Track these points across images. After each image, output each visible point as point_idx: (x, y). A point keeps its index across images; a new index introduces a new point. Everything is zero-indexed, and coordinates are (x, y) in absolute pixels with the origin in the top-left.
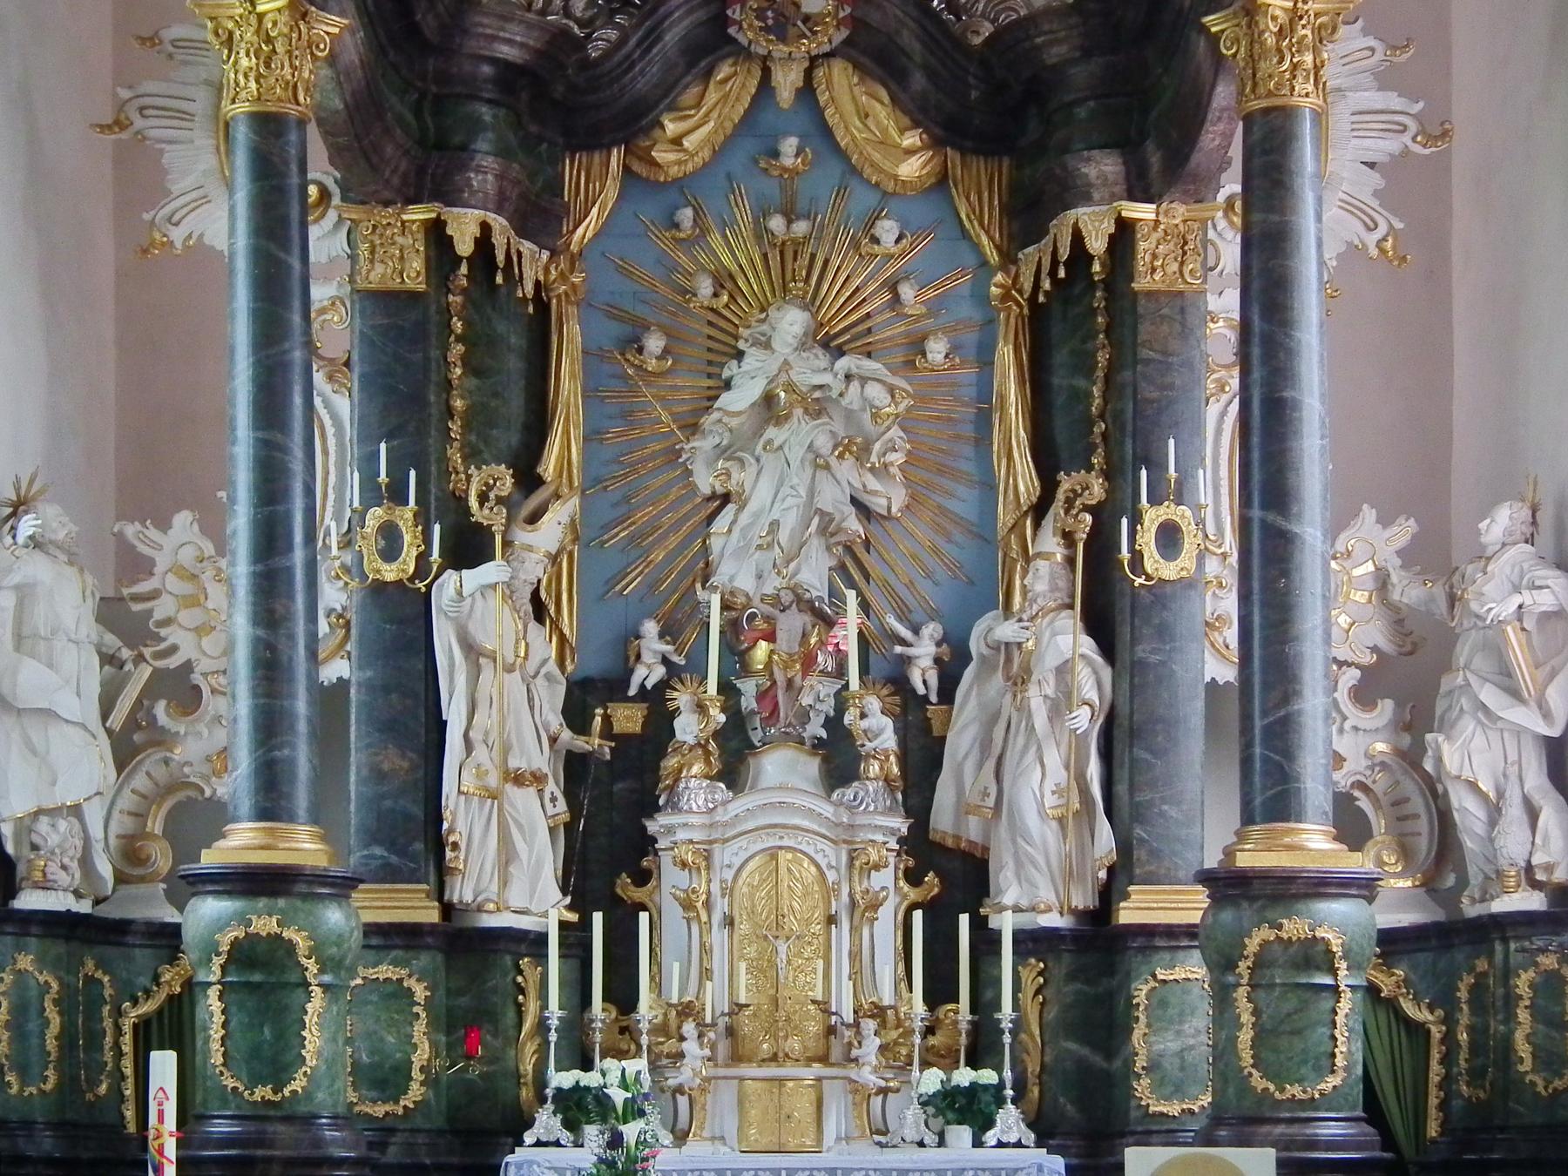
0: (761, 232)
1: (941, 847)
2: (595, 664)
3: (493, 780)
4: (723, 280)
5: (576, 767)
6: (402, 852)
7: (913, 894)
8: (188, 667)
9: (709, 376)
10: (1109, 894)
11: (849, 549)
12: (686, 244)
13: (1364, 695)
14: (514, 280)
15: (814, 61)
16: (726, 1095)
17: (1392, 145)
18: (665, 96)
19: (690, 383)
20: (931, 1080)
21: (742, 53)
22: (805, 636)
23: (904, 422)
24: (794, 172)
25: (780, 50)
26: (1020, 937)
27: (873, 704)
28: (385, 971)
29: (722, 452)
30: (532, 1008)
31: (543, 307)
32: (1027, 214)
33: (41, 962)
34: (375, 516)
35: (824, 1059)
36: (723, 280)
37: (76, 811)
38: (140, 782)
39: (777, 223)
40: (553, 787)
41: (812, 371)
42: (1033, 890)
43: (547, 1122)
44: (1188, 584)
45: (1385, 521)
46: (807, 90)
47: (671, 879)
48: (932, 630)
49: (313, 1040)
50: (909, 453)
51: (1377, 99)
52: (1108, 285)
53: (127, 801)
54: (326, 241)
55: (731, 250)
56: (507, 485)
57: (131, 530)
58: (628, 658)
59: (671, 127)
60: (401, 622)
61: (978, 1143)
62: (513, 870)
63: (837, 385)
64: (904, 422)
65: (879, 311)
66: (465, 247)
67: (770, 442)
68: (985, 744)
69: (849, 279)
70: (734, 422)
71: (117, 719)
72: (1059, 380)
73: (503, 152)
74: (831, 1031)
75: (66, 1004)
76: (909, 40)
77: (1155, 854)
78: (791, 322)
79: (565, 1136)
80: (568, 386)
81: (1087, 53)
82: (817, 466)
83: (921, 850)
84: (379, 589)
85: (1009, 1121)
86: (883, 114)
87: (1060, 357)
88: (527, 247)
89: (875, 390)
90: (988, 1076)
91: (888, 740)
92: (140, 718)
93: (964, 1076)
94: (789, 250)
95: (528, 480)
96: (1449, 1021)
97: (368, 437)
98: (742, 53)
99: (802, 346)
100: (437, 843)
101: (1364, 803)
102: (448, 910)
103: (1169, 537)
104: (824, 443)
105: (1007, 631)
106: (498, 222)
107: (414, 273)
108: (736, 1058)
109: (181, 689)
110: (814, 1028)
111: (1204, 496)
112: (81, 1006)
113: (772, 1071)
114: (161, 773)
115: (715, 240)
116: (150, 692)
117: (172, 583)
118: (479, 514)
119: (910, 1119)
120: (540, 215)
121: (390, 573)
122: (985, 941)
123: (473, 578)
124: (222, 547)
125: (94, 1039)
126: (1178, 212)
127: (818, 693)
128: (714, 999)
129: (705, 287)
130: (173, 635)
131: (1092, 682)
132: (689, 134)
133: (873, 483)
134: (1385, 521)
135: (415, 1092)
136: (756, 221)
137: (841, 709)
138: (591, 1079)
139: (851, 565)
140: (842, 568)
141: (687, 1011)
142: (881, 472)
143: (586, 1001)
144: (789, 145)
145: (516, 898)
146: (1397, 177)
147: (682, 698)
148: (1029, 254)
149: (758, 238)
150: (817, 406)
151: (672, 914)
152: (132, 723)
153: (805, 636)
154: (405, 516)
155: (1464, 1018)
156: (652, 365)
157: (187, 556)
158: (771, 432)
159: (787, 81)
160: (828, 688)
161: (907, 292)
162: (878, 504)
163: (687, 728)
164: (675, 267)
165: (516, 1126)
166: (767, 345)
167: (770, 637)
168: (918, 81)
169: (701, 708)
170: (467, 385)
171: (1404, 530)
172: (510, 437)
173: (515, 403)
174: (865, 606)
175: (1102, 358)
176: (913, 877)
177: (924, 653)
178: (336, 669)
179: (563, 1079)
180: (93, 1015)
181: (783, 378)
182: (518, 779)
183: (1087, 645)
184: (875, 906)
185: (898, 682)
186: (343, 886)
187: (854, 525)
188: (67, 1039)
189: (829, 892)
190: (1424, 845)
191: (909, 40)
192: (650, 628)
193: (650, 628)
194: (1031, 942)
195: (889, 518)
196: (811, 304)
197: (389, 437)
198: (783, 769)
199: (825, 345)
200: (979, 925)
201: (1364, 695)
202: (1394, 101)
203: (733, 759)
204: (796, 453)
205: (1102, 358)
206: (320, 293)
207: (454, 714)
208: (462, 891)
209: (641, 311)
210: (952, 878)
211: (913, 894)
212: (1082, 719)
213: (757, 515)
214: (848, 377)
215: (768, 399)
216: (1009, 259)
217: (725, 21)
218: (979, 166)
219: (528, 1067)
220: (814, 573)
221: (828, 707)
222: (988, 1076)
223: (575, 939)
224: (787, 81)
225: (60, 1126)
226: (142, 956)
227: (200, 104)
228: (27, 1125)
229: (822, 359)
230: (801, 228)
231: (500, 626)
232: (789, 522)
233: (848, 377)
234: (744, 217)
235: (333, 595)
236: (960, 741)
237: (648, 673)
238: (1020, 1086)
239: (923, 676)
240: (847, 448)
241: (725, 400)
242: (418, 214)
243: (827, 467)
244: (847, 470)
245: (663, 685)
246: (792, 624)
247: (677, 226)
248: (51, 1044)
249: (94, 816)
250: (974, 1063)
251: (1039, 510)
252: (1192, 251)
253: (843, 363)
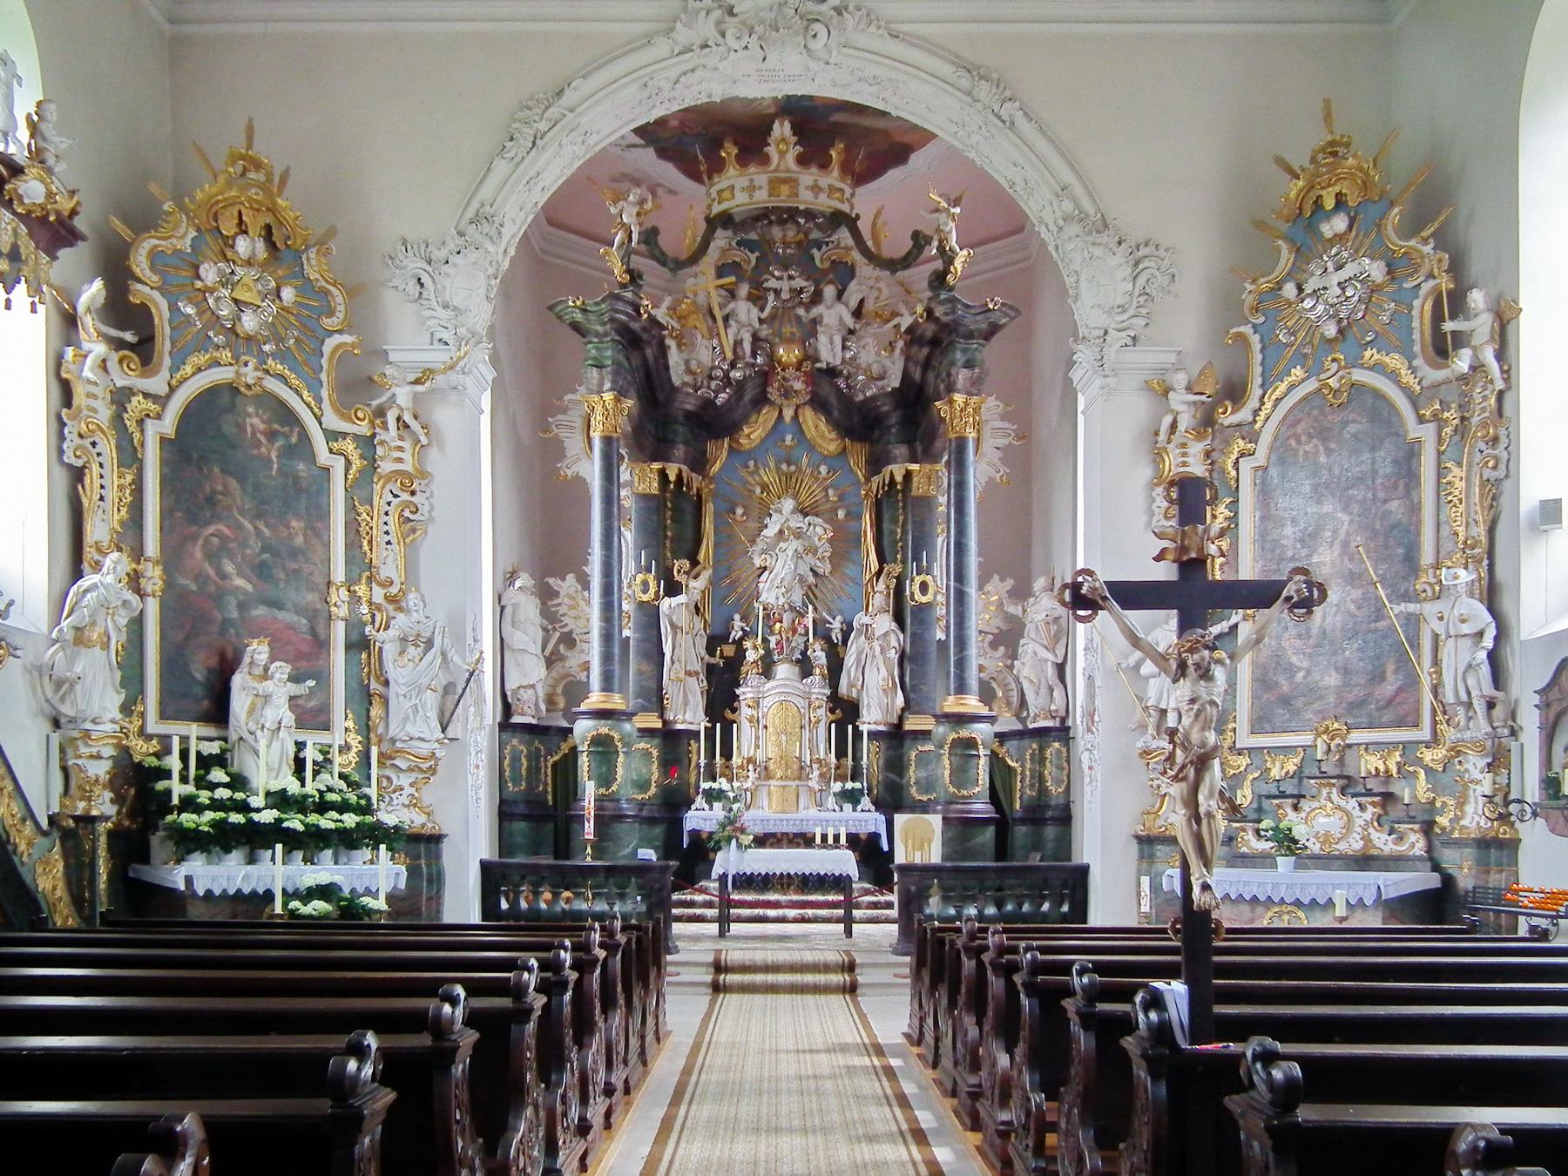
0: (778, 469)
1: (842, 699)
2: (718, 630)
3: (682, 674)
4: (765, 487)
5: (710, 669)
6: (649, 701)
7: (832, 717)
8: (571, 632)
10: (901, 718)
12: (751, 474)
13: (994, 645)
14: (689, 488)
15: (798, 407)
16: (765, 792)
17: (1005, 441)
18: (745, 419)
19: (752, 525)
20: (837, 787)
21: (772, 403)
23: (830, 541)
24: (791, 447)
25: (785, 403)
26: (869, 733)
27: (817, 646)
28: (642, 745)
30: (694, 758)
31: (699, 496)
32: (875, 464)
33: (520, 742)
34: (640, 577)
35: (800, 778)
36: (765, 487)
37: (533, 686)
38: (554, 674)
39: (784, 467)
40: (701, 676)
41: (797, 522)
42: (872, 718)
43: (700, 801)
44: (929, 605)
45: (1002, 580)
46: (796, 417)
47: (745, 711)
48: (839, 618)
49: (620, 770)
51: (1000, 424)
52: (903, 491)
53: (550, 681)
54: (625, 476)
55: (768, 476)
56: (686, 564)
57: (551, 581)
58: (729, 629)
59: (746, 431)
60: (650, 616)
61: (854, 810)
62: (689, 713)
64: (830, 541)
66: (672, 478)
68: (858, 660)
69: (810, 490)
71: (547, 653)
72: (886, 526)
73: (686, 443)
74: (802, 768)
75: (528, 757)
76: (833, 400)
77: (919, 704)
78: (788, 504)
79: (707, 807)
80: (708, 526)
81: (896, 409)
83: (835, 701)
84: (641, 604)
85: (866, 802)
86: (823, 426)
87: (886, 517)
88: (694, 475)
89: (820, 531)
90: (858, 785)
91: (824, 661)
92: (555, 652)
93: (849, 785)
94: (789, 476)
95: (695, 563)
96: (1022, 766)
97: (638, 548)
98: (772, 403)
99: (793, 512)
100: (661, 698)
101: (994, 685)
102: (665, 722)
103: (924, 587)
104: (801, 549)
105: (866, 620)
106: (684, 468)
107: (654, 487)
108: (768, 777)
109: (569, 640)
110: (796, 767)
111: (936, 572)
112: (534, 757)
113: (780, 783)
114: (562, 671)
115: (762, 472)
116: (559, 641)
117: (566, 600)
118: (677, 578)
119: (831, 802)
120: (699, 463)
121: (645, 598)
122: (858, 734)
123: (675, 601)
124: (586, 585)
125: (538, 770)
126: (927, 467)
127: (798, 641)
128: (760, 756)
129: (758, 490)
130: (566, 620)
131: (896, 640)
132: (754, 433)
134: (1002, 580)
135: (653, 790)
137: (806, 649)
138: (715, 786)
141: (750, 760)
142: (822, 559)
143: (714, 757)
144: (789, 438)
145: (688, 716)
146: (1007, 453)
147: (748, 644)
148: (876, 479)
150: (798, 535)
151: (745, 725)
152: (552, 653)
154: (651, 578)
155: (1028, 765)
156: (739, 518)
157: (572, 591)
158: (782, 545)
159: (788, 414)
160: (801, 640)
161: (831, 492)
162: (821, 571)
163: (751, 656)
165: (688, 803)
168: (836, 413)
169: (755, 647)
170: (676, 527)
171: (1010, 583)
172: (687, 546)
173: (689, 533)
174: (815, 609)
175: (901, 518)
176: (832, 711)
177: (836, 625)
178: (626, 633)
179: (705, 785)
180: (538, 761)
182: (688, 673)
183: (894, 625)
184: (818, 722)
185: (827, 638)
186: (629, 716)
187: (811, 579)
188: (529, 769)
189: (802, 716)
190: (1015, 699)
191: (833, 400)
192: (737, 617)
193: (737, 617)
194: (873, 735)
196: (795, 497)
197: (645, 547)
198: (784, 671)
200: (856, 728)
201: (994, 645)
202: (1007, 425)
203: (767, 670)
204: (790, 553)
205: (901, 518)
206: (623, 493)
207: (667, 649)
208: (670, 716)
210: (845, 710)
211: (832, 717)
212: (893, 655)
215: (781, 532)
216: (868, 480)
217: (764, 392)
218: (858, 446)
219: (693, 780)
220: (797, 598)
221: (802, 647)
222: (858, 785)
223: (710, 733)
224: (788, 414)
225: (528, 803)
226: (556, 739)
227: (579, 423)
228: (515, 802)
230: (793, 468)
231: (683, 618)
232: (789, 578)
234: (772, 464)
235: (625, 607)
236: (850, 660)
237: (736, 634)
238: (870, 789)
239: (836, 636)
242: (656, 466)
244: (809, 559)
245: (742, 639)
246: (787, 617)
248: (524, 772)
249: (539, 687)
250: (853, 780)
251: (879, 574)
252: (931, 480)
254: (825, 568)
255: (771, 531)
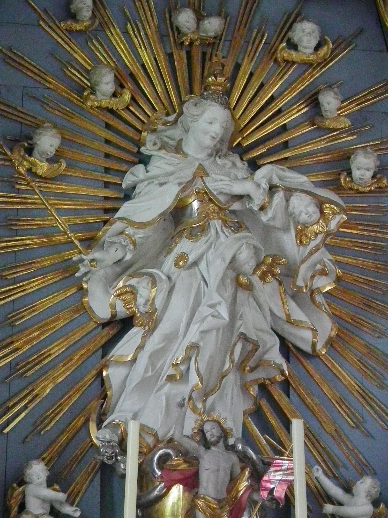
9: (107, 185)
11: (263, 387)
22: (233, 480)
29: (123, 268)
39: (185, 19)
41: (228, 179)
48: (366, 486)
50: (338, 280)
63: (259, 198)
65: (297, 124)
67: (183, 256)
70: (139, 235)
78: (208, 121)
82: (238, 285)
99: (216, 153)
104: (246, 258)
129: (106, 83)
133: (298, 314)
136: (162, 18)
139: (269, 410)
140: (257, 414)
142: (305, 297)
149: (163, 37)
153: (233, 480)
156: (43, 168)
158: (183, 245)
161: (330, 101)
162: (303, 338)
164: (72, 62)
166: (178, 149)
167: (191, 482)
181: (199, 184)
192: (38, 471)
193: (38, 471)
195: (312, 356)
199: (241, 151)
204: (214, 269)
209: (31, 107)
213: (170, 338)
214: (272, 189)
215: (178, 213)
229: (242, 168)
230: (213, 25)
232: (210, 347)
233: (272, 189)
240: (270, 271)
241: (125, 209)
243: (249, 287)
247: (73, 17)
253: (261, 174)
254: (315, 329)
255: (149, 203)
